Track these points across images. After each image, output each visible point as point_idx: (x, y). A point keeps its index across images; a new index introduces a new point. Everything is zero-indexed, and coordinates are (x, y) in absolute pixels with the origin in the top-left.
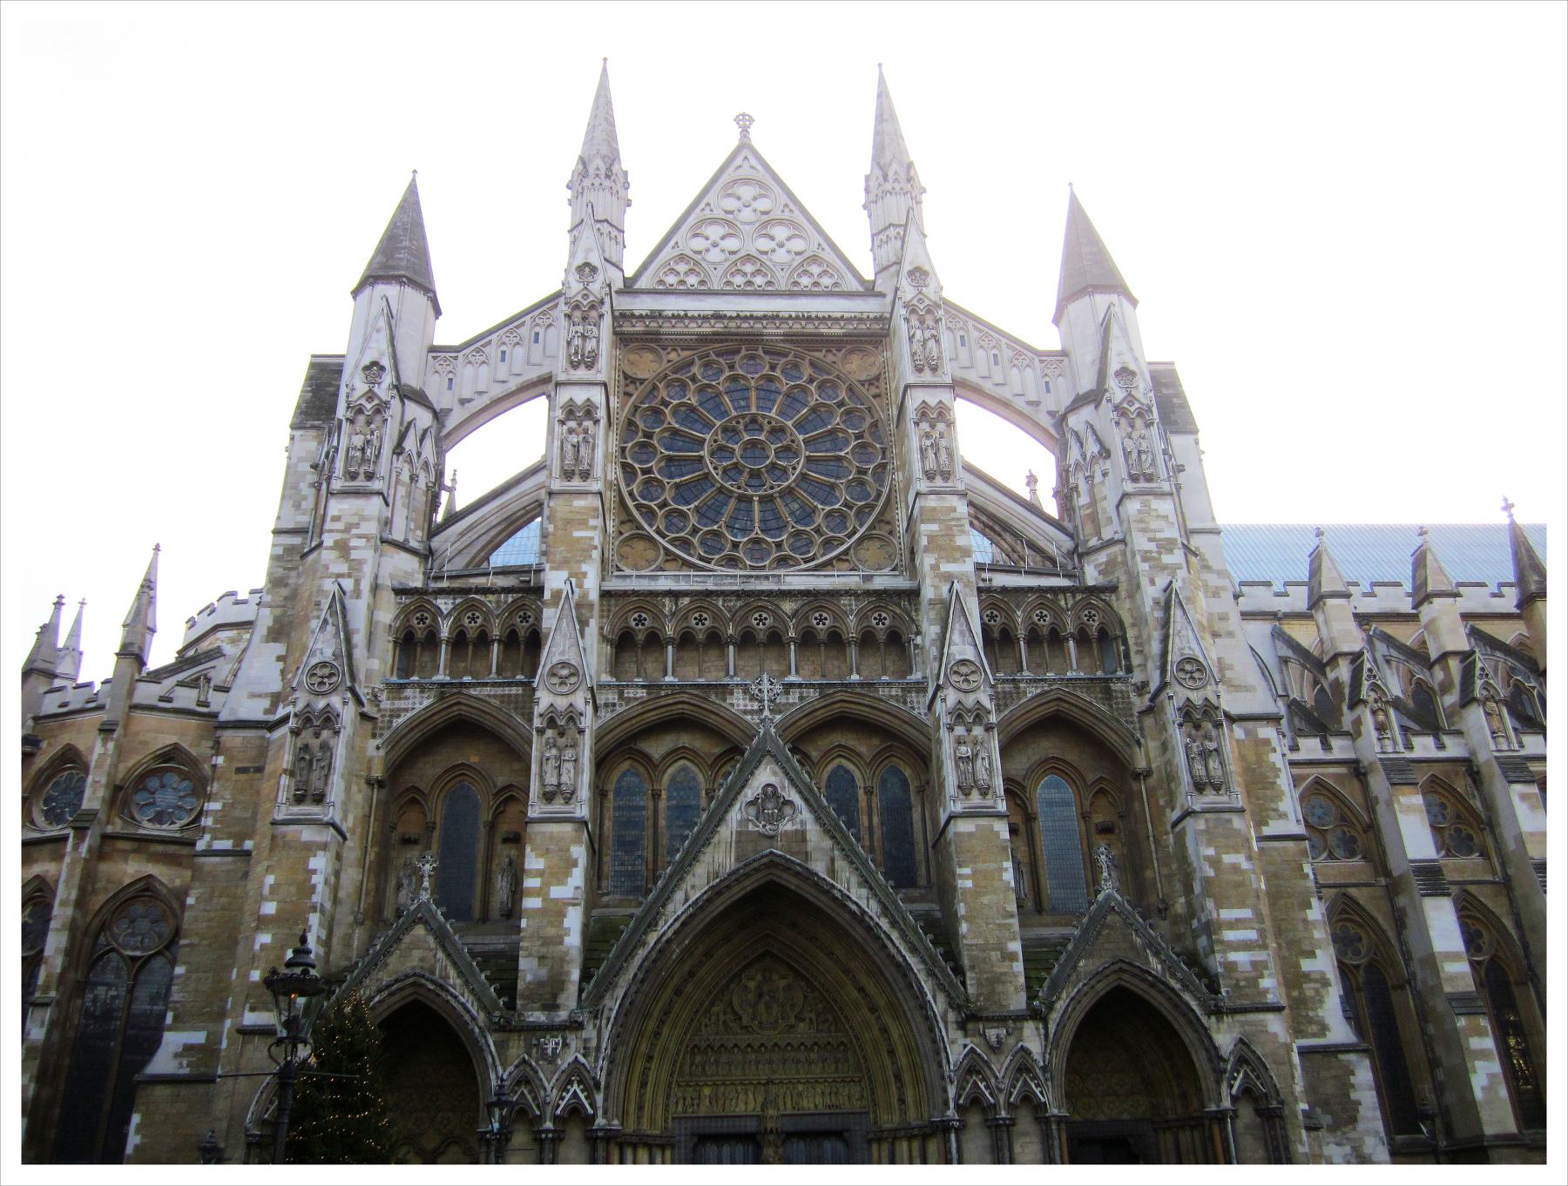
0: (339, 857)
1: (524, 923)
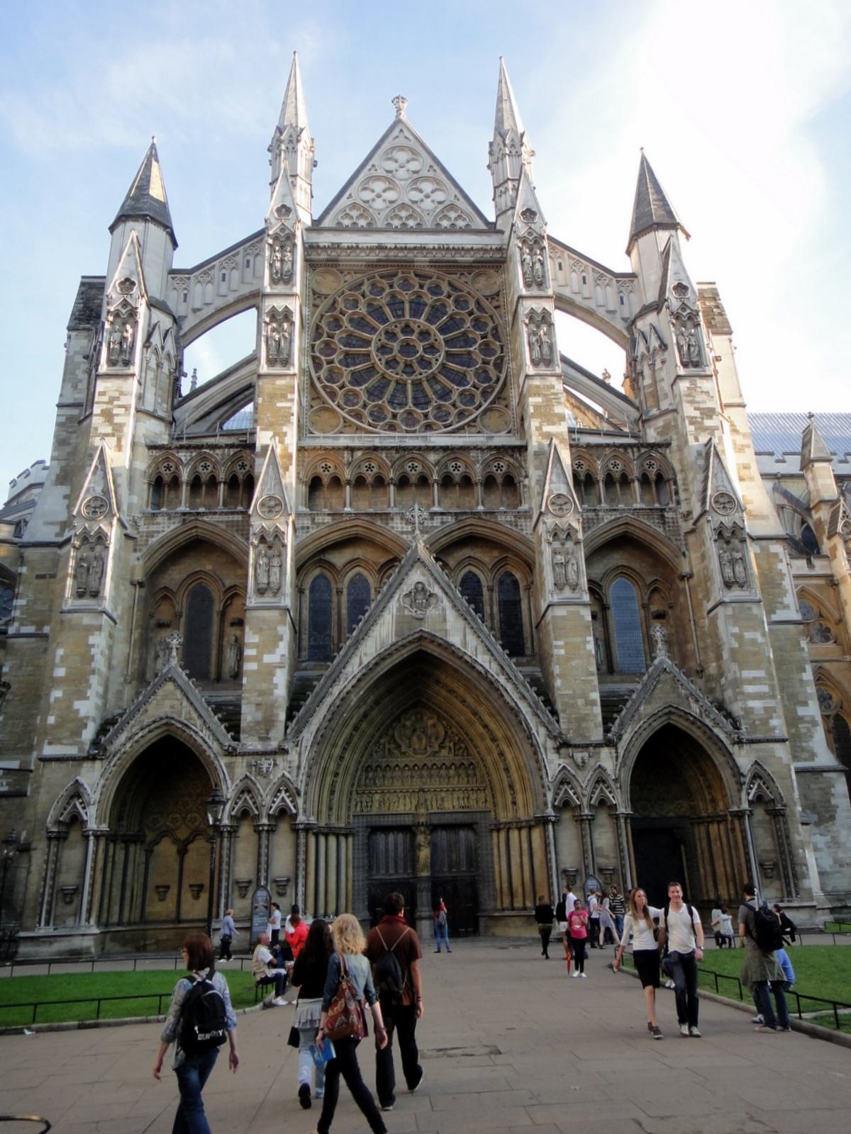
0: (111, 636)
1: (245, 680)
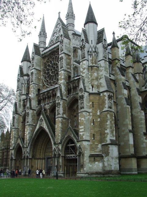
0: (17, 131)
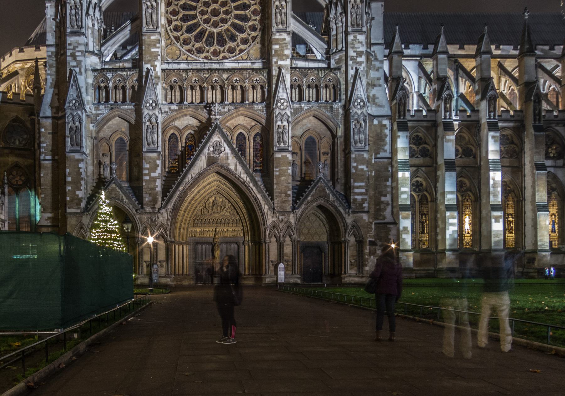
0: (86, 163)
1: (144, 184)
